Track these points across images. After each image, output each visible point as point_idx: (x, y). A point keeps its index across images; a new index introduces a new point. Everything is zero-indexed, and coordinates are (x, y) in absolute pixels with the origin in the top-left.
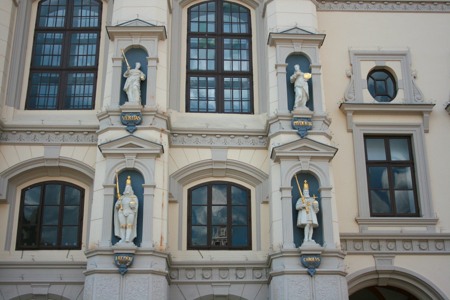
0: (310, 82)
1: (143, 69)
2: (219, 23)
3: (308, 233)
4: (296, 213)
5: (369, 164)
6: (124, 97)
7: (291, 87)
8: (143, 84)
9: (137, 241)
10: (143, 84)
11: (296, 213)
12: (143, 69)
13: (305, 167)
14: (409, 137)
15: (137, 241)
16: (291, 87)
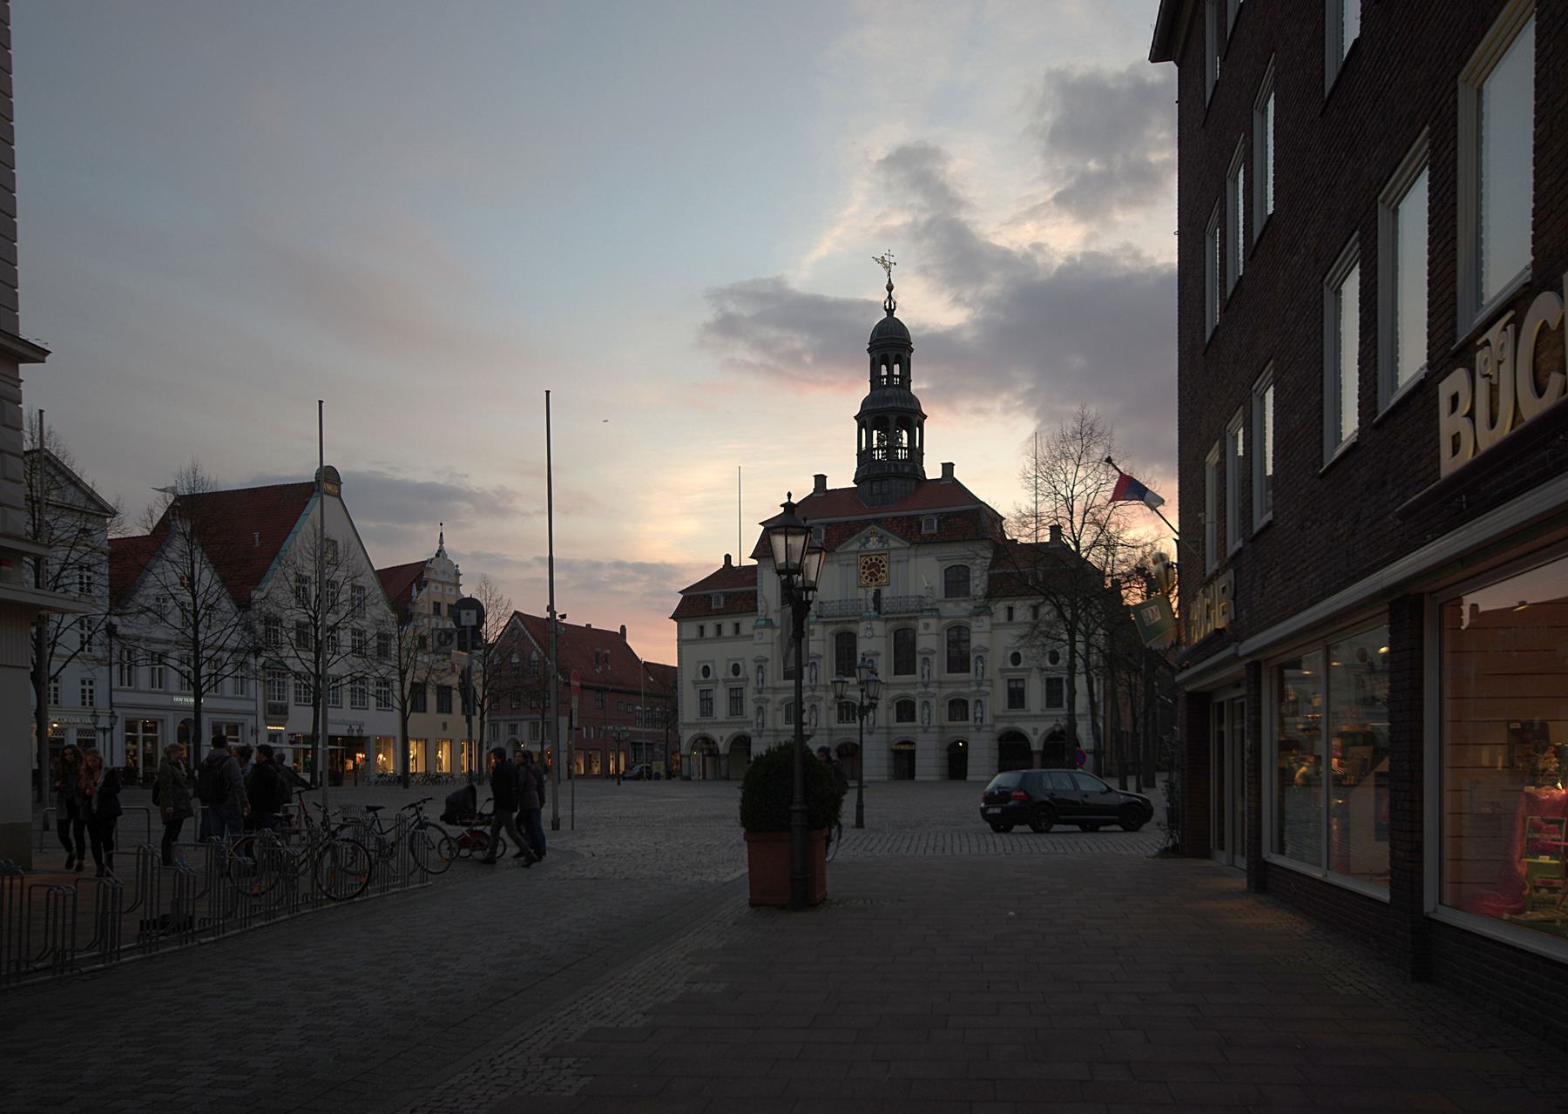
0: (983, 668)
1: (929, 665)
2: (959, 634)
3: (978, 720)
4: (975, 714)
5: (1009, 689)
6: (923, 676)
7: (977, 669)
8: (929, 671)
9: (929, 723)
10: (929, 671)
11: (975, 714)
12: (929, 665)
13: (978, 698)
14: (1023, 680)
15: (929, 723)
16: (977, 669)
